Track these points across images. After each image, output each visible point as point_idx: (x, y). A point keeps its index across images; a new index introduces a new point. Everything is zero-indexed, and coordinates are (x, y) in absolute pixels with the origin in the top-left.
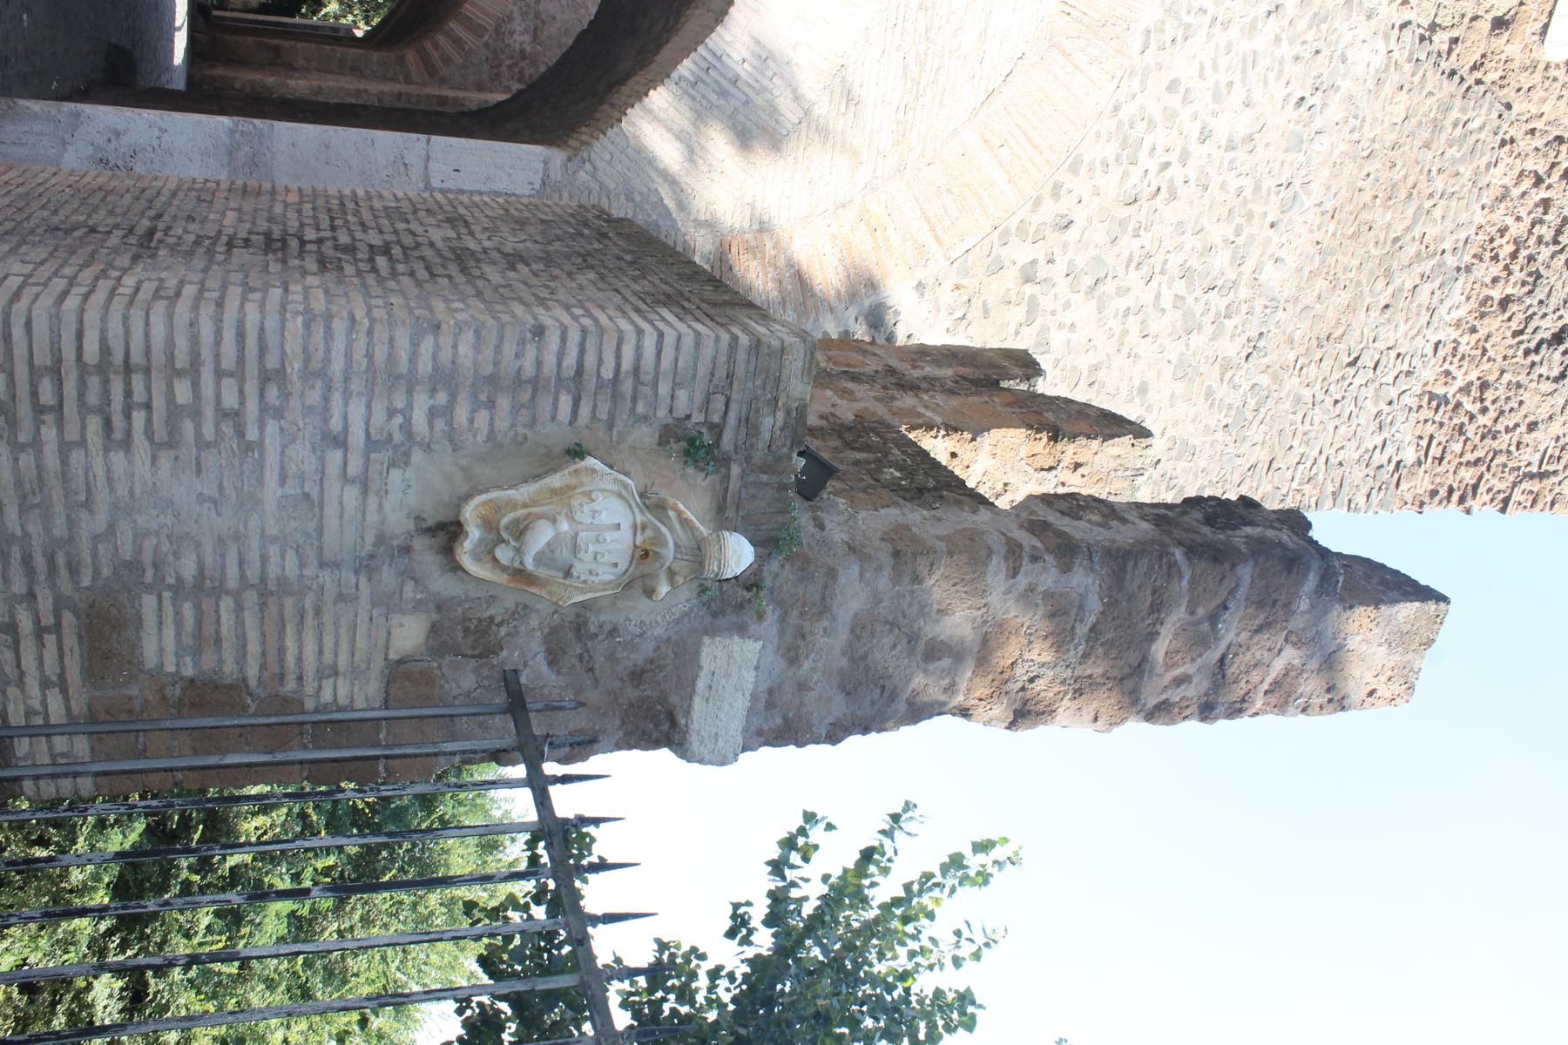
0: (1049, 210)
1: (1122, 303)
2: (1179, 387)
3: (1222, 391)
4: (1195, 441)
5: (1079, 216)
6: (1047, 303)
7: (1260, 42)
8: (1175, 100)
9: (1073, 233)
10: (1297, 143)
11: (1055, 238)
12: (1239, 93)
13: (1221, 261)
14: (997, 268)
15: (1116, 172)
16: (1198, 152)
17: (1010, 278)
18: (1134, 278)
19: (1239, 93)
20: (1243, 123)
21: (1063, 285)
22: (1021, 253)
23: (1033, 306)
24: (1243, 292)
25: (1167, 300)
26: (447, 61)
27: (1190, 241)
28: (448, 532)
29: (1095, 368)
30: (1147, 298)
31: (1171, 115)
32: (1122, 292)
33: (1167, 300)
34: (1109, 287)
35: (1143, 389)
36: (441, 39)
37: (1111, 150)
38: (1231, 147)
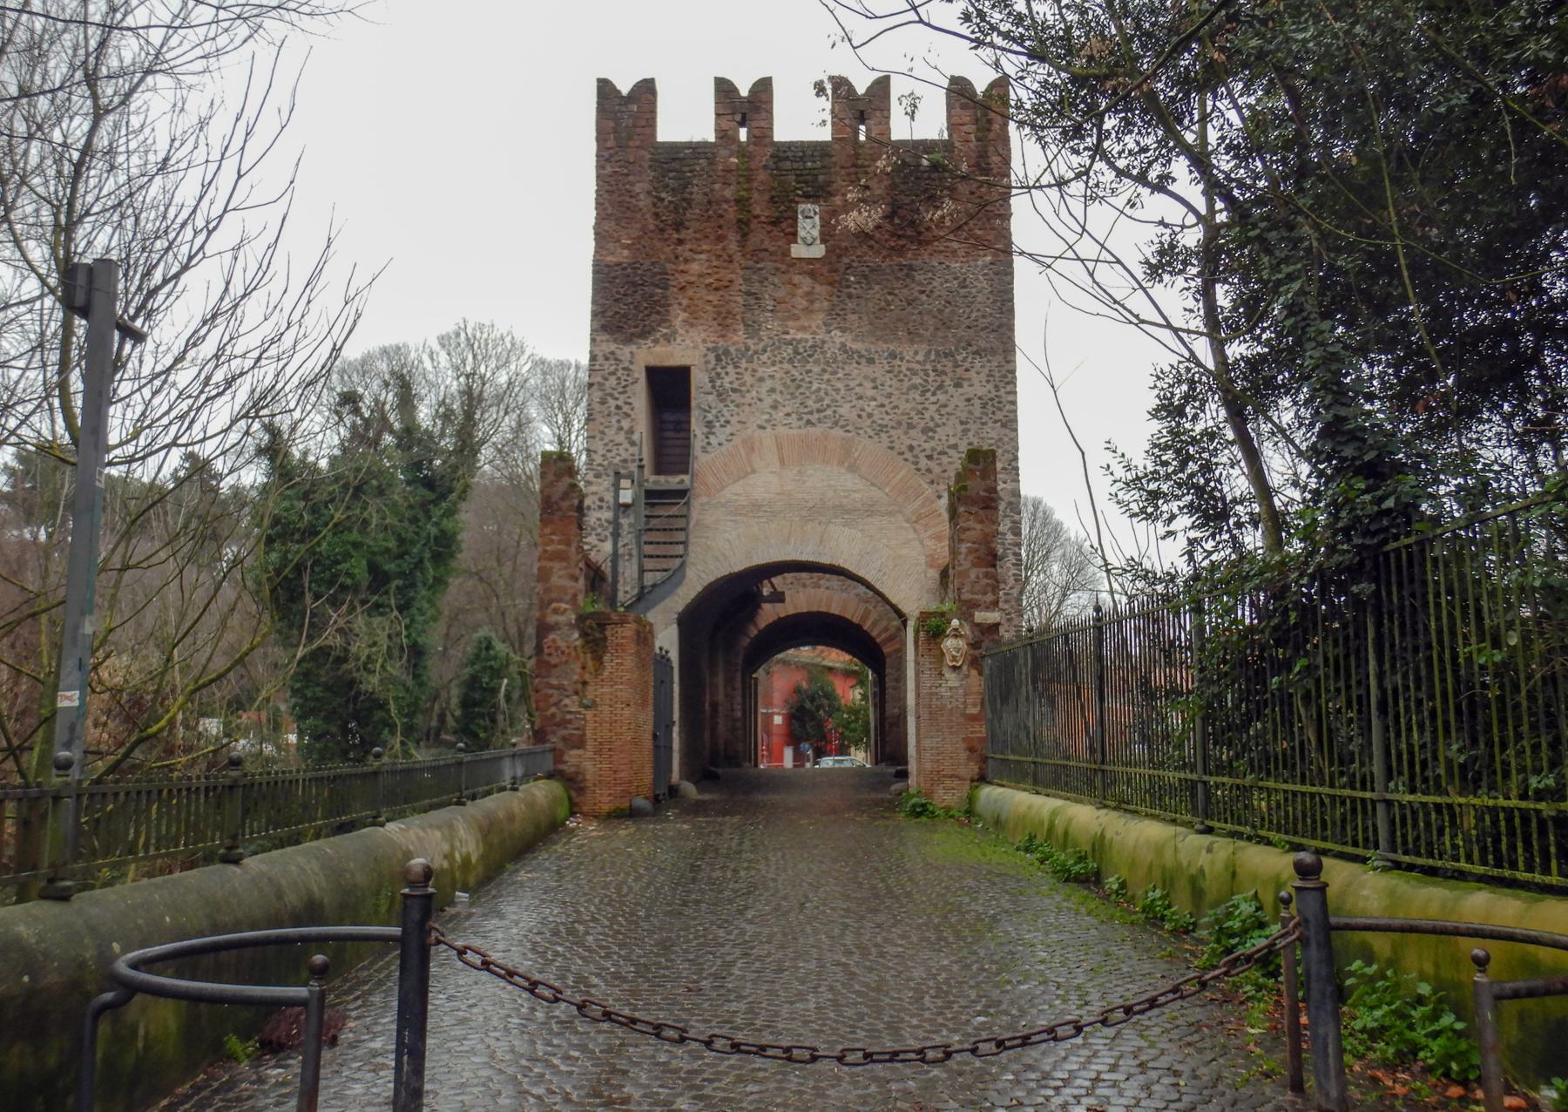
0: (908, 455)
1: (937, 417)
2: (965, 384)
3: (967, 365)
4: (986, 371)
5: (909, 442)
6: (939, 449)
7: (839, 385)
8: (864, 414)
9: (914, 443)
10: (871, 361)
11: (916, 451)
12: (858, 389)
13: (917, 380)
14: (929, 470)
15: (893, 432)
16: (881, 400)
17: (932, 464)
18: (927, 415)
19: (858, 389)
20: (869, 385)
21: (933, 444)
22: (924, 463)
23: (942, 453)
24: (928, 366)
25: (933, 399)
26: (886, 629)
27: (911, 396)
28: (954, 668)
29: (962, 423)
30: (934, 408)
31: (870, 415)
32: (932, 419)
33: (933, 399)
34: (931, 424)
35: (968, 400)
36: (874, 634)
37: (883, 435)
38: (875, 388)
